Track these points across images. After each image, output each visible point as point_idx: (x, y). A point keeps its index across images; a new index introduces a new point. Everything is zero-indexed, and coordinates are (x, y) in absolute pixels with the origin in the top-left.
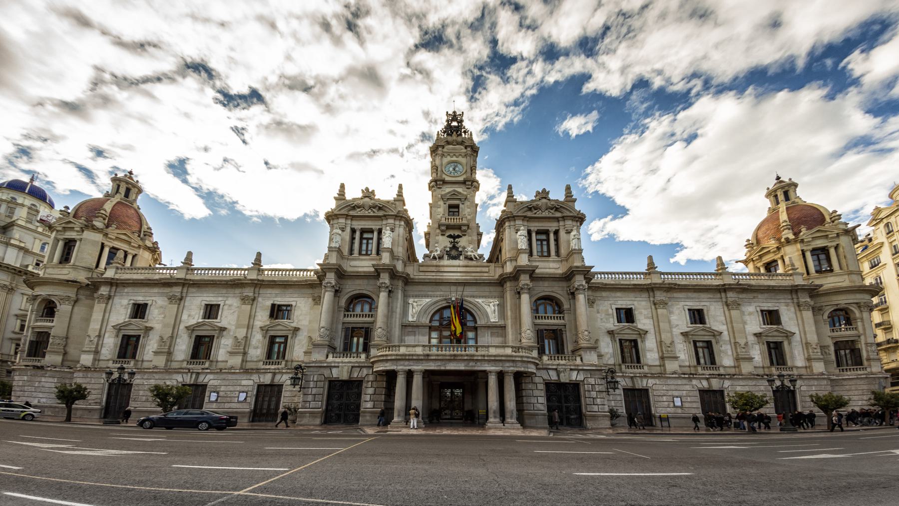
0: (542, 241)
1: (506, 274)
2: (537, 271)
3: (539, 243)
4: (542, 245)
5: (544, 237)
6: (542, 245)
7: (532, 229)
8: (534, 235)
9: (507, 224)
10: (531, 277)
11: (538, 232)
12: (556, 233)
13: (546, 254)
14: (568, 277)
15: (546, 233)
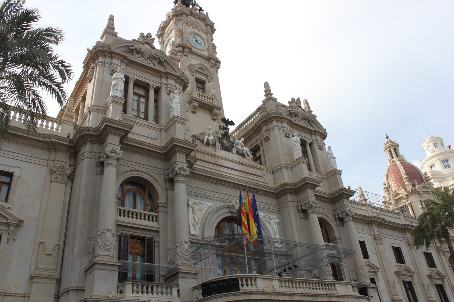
0: (139, 96)
1: (88, 129)
2: (130, 135)
3: (136, 98)
4: (139, 102)
5: (142, 92)
6: (139, 102)
7: (130, 76)
8: (131, 85)
9: (101, 59)
10: (121, 142)
11: (138, 84)
12: (157, 91)
13: (142, 116)
14: (167, 154)
15: (145, 87)
